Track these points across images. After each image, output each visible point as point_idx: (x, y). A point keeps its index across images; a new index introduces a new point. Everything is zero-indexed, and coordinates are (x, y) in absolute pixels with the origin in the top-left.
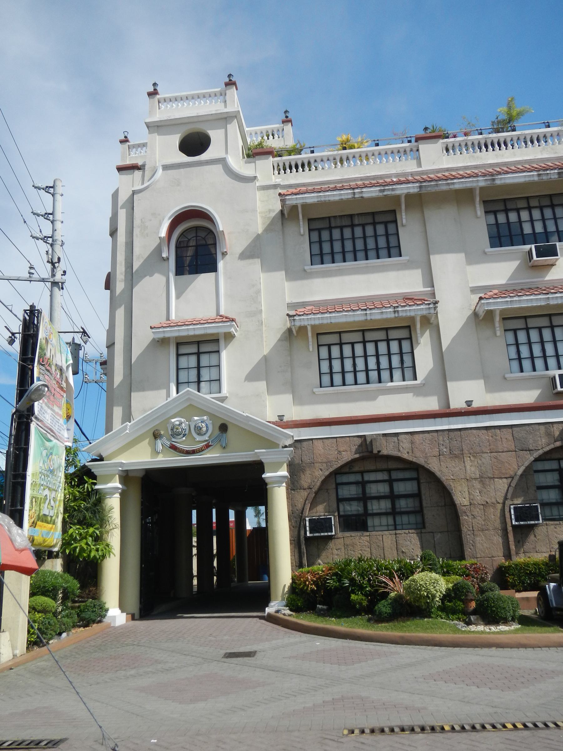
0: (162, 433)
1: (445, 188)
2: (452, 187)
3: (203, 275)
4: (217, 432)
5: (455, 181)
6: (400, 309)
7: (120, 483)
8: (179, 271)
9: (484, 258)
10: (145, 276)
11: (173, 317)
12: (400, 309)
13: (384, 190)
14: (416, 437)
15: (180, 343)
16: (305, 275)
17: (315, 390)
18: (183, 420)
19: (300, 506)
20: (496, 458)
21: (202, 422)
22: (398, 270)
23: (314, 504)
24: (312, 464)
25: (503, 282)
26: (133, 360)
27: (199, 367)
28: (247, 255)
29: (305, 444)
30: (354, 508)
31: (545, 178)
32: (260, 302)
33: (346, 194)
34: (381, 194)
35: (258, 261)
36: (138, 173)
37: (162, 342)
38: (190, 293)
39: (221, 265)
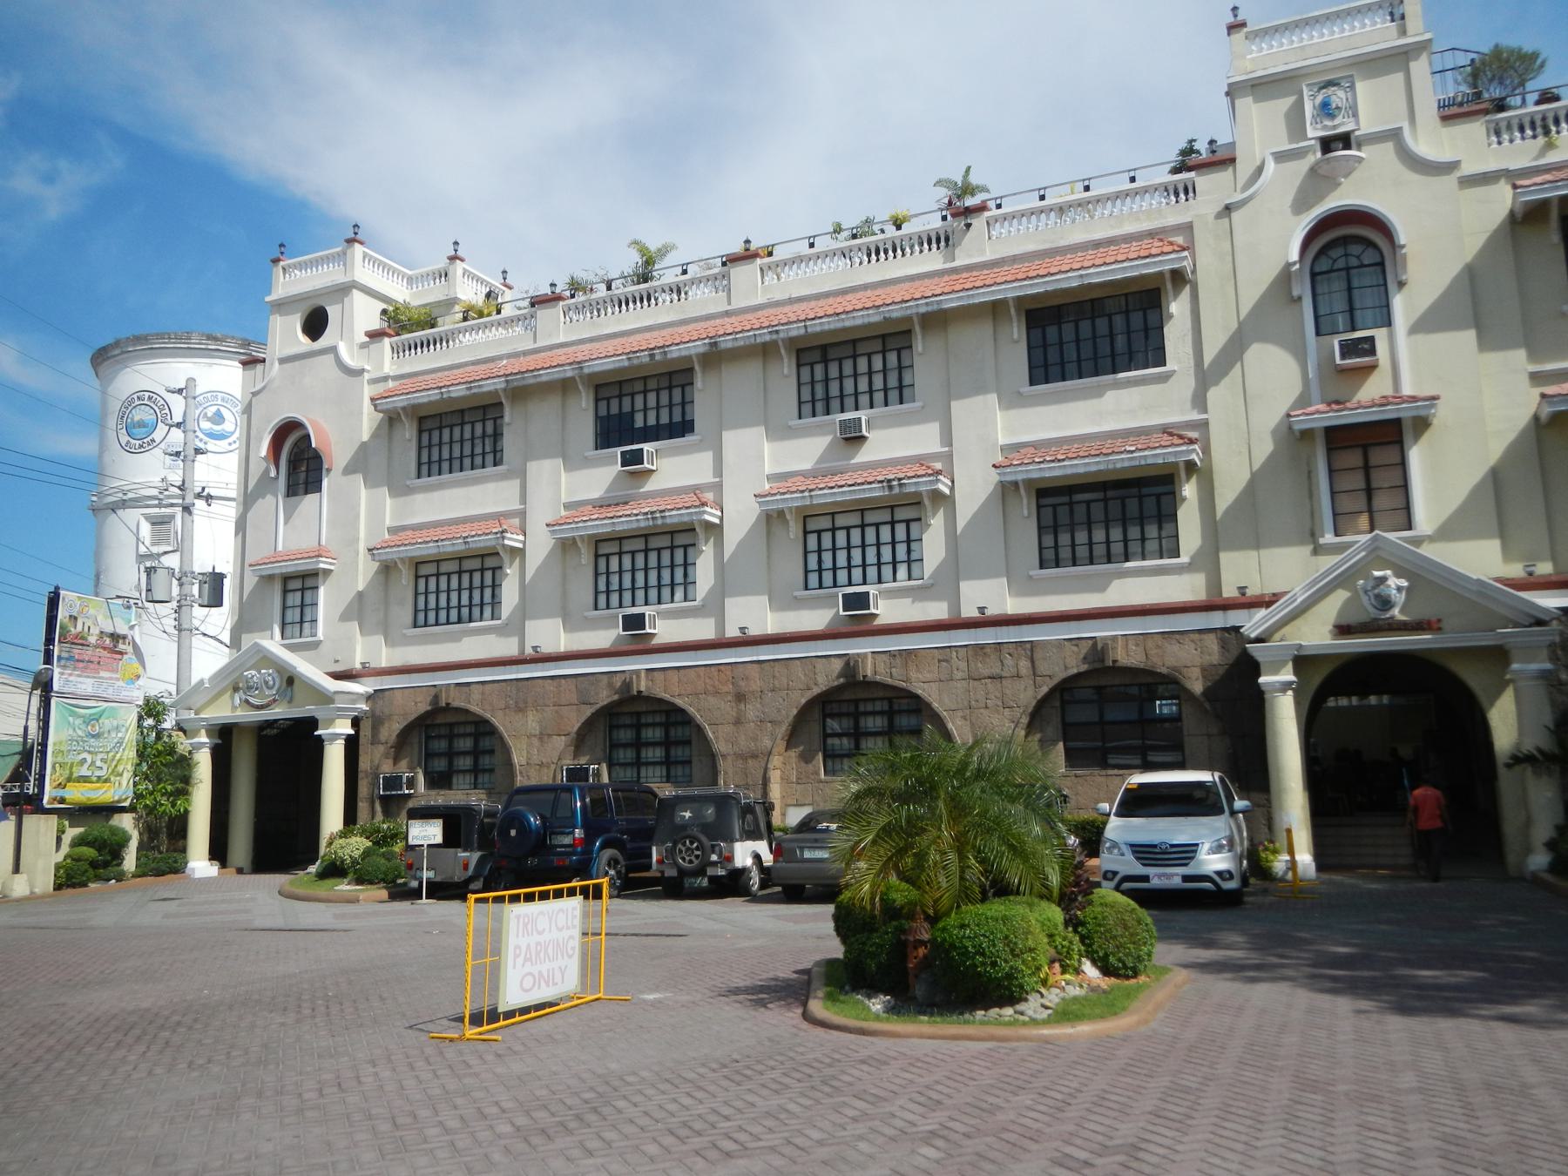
0: (241, 685)
1: (532, 381)
2: (539, 380)
3: (309, 496)
4: (285, 684)
5: (541, 372)
6: (469, 540)
7: (209, 736)
8: (292, 491)
9: (587, 463)
10: (258, 498)
11: (280, 548)
12: (469, 540)
13: (470, 388)
14: (488, 687)
15: (286, 579)
16: (409, 491)
17: (405, 631)
18: (253, 672)
19: (377, 762)
20: (557, 712)
21: (269, 675)
22: (497, 481)
23: (396, 760)
24: (390, 717)
25: (596, 496)
26: (245, 598)
27: (302, 606)
28: (348, 470)
29: (387, 693)
30: (440, 765)
31: (635, 362)
32: (357, 529)
33: (434, 395)
34: (468, 393)
35: (359, 478)
36: (259, 367)
37: (268, 579)
38: (297, 519)
39: (325, 483)
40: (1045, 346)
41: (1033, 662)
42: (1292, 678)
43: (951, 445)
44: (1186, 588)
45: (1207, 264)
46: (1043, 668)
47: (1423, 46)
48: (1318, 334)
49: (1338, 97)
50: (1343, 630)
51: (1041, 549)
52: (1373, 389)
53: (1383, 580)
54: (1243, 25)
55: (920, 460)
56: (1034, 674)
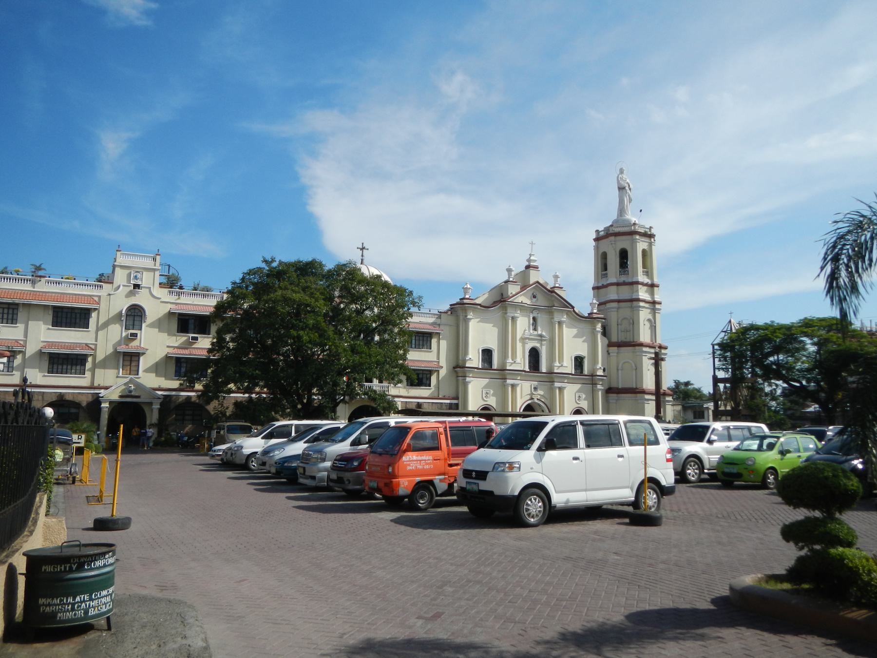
40: (57, 317)
41: (43, 397)
42: (108, 406)
43: (26, 338)
44: (83, 381)
45: (103, 307)
46: (45, 398)
47: (158, 270)
48: (125, 329)
49: (139, 275)
50: (121, 397)
51: (48, 368)
52: (135, 343)
53: (131, 387)
54: (120, 251)
55: (17, 341)
56: (43, 400)
